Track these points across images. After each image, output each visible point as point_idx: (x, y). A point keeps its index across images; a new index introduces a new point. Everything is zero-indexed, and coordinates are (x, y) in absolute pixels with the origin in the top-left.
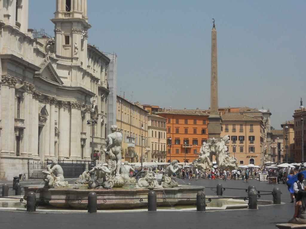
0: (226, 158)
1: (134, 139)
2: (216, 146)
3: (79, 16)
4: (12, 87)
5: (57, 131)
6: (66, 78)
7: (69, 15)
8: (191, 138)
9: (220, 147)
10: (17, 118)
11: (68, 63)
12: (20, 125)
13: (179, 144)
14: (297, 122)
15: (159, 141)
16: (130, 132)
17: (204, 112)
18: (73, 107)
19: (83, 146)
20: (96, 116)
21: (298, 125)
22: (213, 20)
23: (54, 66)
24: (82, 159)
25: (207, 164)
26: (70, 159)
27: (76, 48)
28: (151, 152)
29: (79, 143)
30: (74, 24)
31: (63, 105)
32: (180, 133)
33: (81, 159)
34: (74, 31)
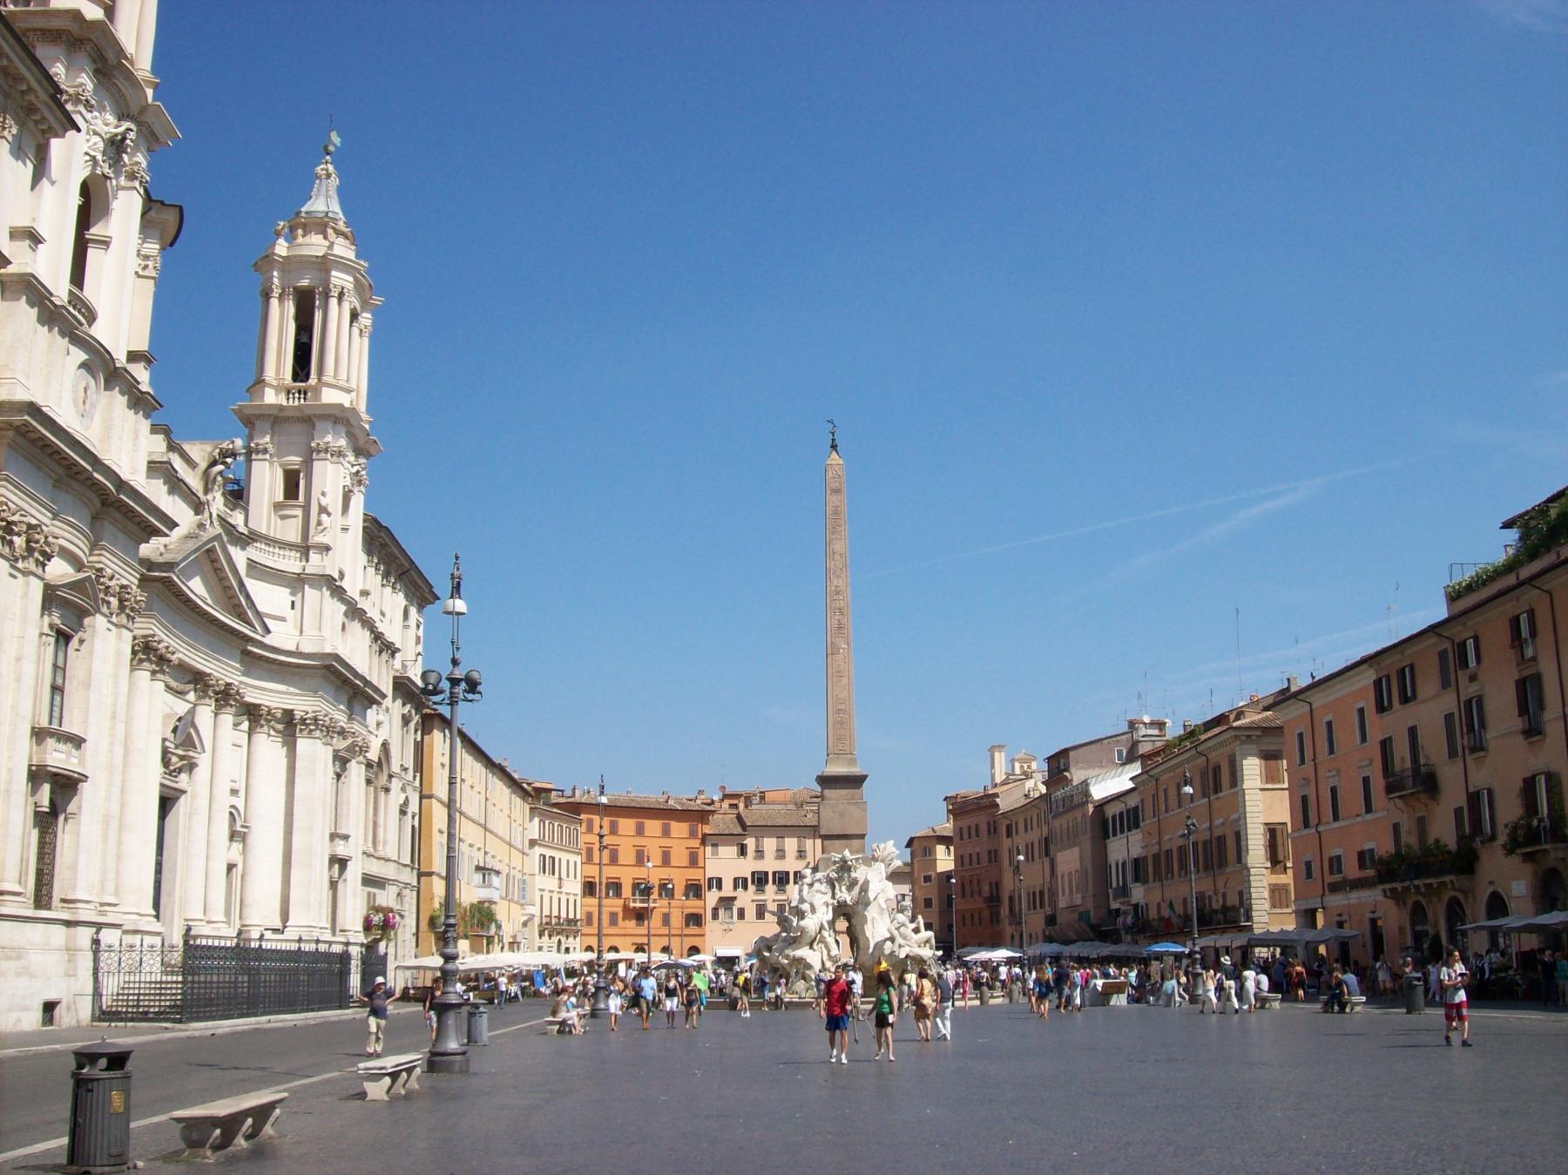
3: (345, 400)
4: (26, 573)
5: (239, 823)
6: (283, 619)
7: (302, 396)
10: (44, 723)
11: (290, 563)
12: (58, 757)
13: (618, 894)
14: (961, 829)
15: (560, 888)
16: (483, 851)
17: (691, 800)
18: (301, 730)
21: (965, 836)
23: (240, 556)
24: (334, 934)
26: (291, 933)
27: (323, 510)
28: (537, 921)
29: (321, 872)
31: (263, 722)
32: (620, 863)
33: (327, 936)
34: (319, 452)
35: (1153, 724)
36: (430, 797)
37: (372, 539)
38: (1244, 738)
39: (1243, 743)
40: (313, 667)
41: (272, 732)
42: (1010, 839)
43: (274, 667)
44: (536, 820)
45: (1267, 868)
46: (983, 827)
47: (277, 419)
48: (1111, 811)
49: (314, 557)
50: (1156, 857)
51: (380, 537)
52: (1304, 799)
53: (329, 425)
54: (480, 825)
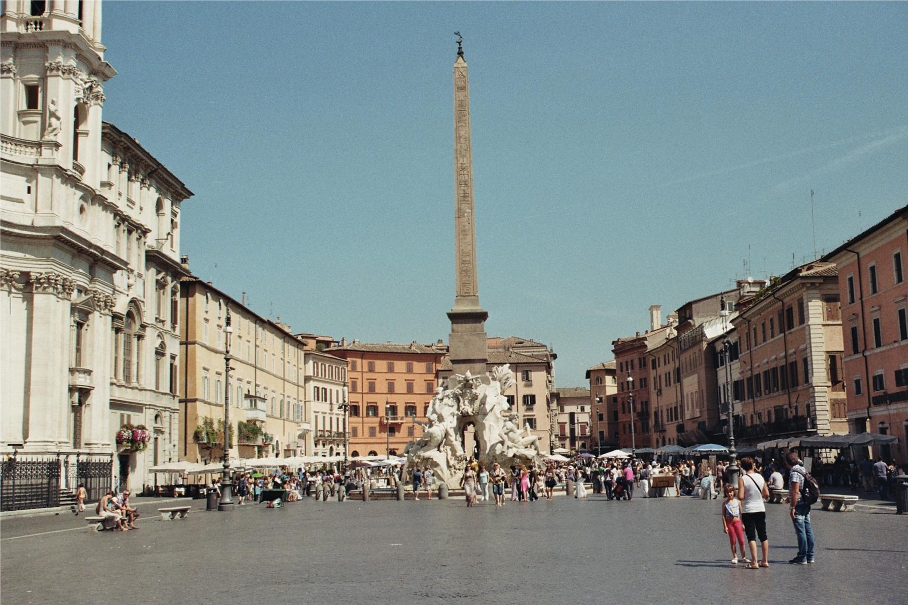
0: (507, 431)
1: (264, 400)
2: (474, 398)
6: (21, 201)
7: (38, 26)
8: (400, 403)
9: (488, 400)
11: (27, 157)
13: (376, 414)
14: (621, 363)
15: (331, 410)
16: (253, 384)
17: (428, 347)
18: (37, 288)
19: (77, 410)
20: (136, 328)
21: (624, 368)
22: (457, 38)
24: (76, 444)
25: (450, 453)
26: (27, 448)
27: (53, 114)
28: (313, 434)
30: (52, 49)
33: (69, 448)
34: (52, 70)
35: (755, 283)
36: (194, 343)
37: (114, 142)
38: (809, 285)
39: (808, 288)
40: (45, 238)
41: (13, 290)
42: (655, 370)
43: (11, 238)
44: (311, 362)
45: (828, 387)
46: (636, 362)
47: (16, 45)
48: (719, 347)
49: (46, 152)
50: (750, 380)
51: (122, 141)
52: (854, 330)
53: (59, 49)
54: (250, 365)
